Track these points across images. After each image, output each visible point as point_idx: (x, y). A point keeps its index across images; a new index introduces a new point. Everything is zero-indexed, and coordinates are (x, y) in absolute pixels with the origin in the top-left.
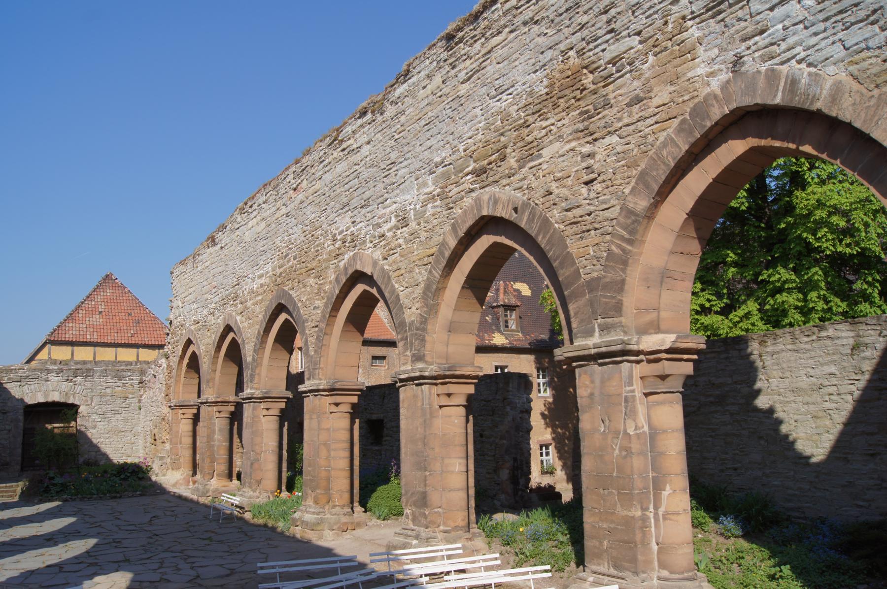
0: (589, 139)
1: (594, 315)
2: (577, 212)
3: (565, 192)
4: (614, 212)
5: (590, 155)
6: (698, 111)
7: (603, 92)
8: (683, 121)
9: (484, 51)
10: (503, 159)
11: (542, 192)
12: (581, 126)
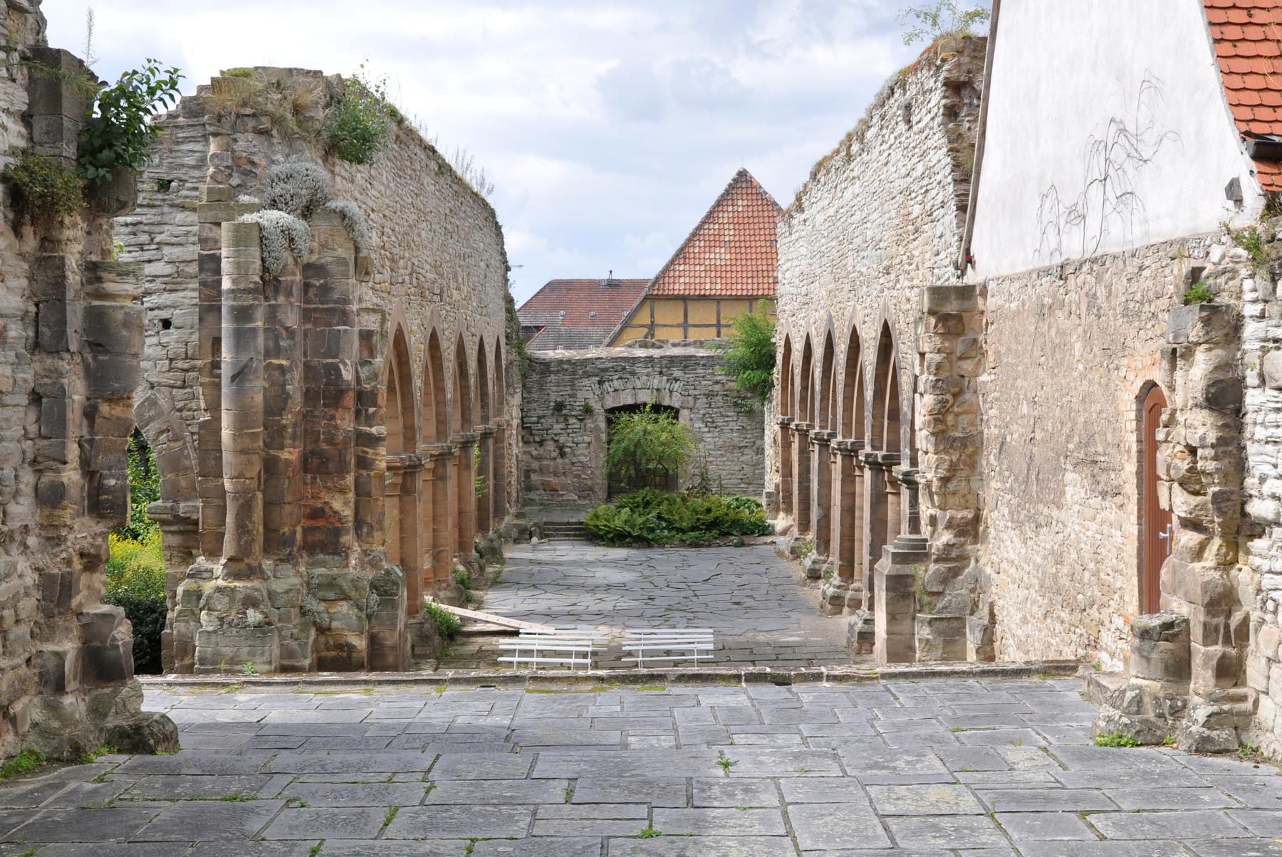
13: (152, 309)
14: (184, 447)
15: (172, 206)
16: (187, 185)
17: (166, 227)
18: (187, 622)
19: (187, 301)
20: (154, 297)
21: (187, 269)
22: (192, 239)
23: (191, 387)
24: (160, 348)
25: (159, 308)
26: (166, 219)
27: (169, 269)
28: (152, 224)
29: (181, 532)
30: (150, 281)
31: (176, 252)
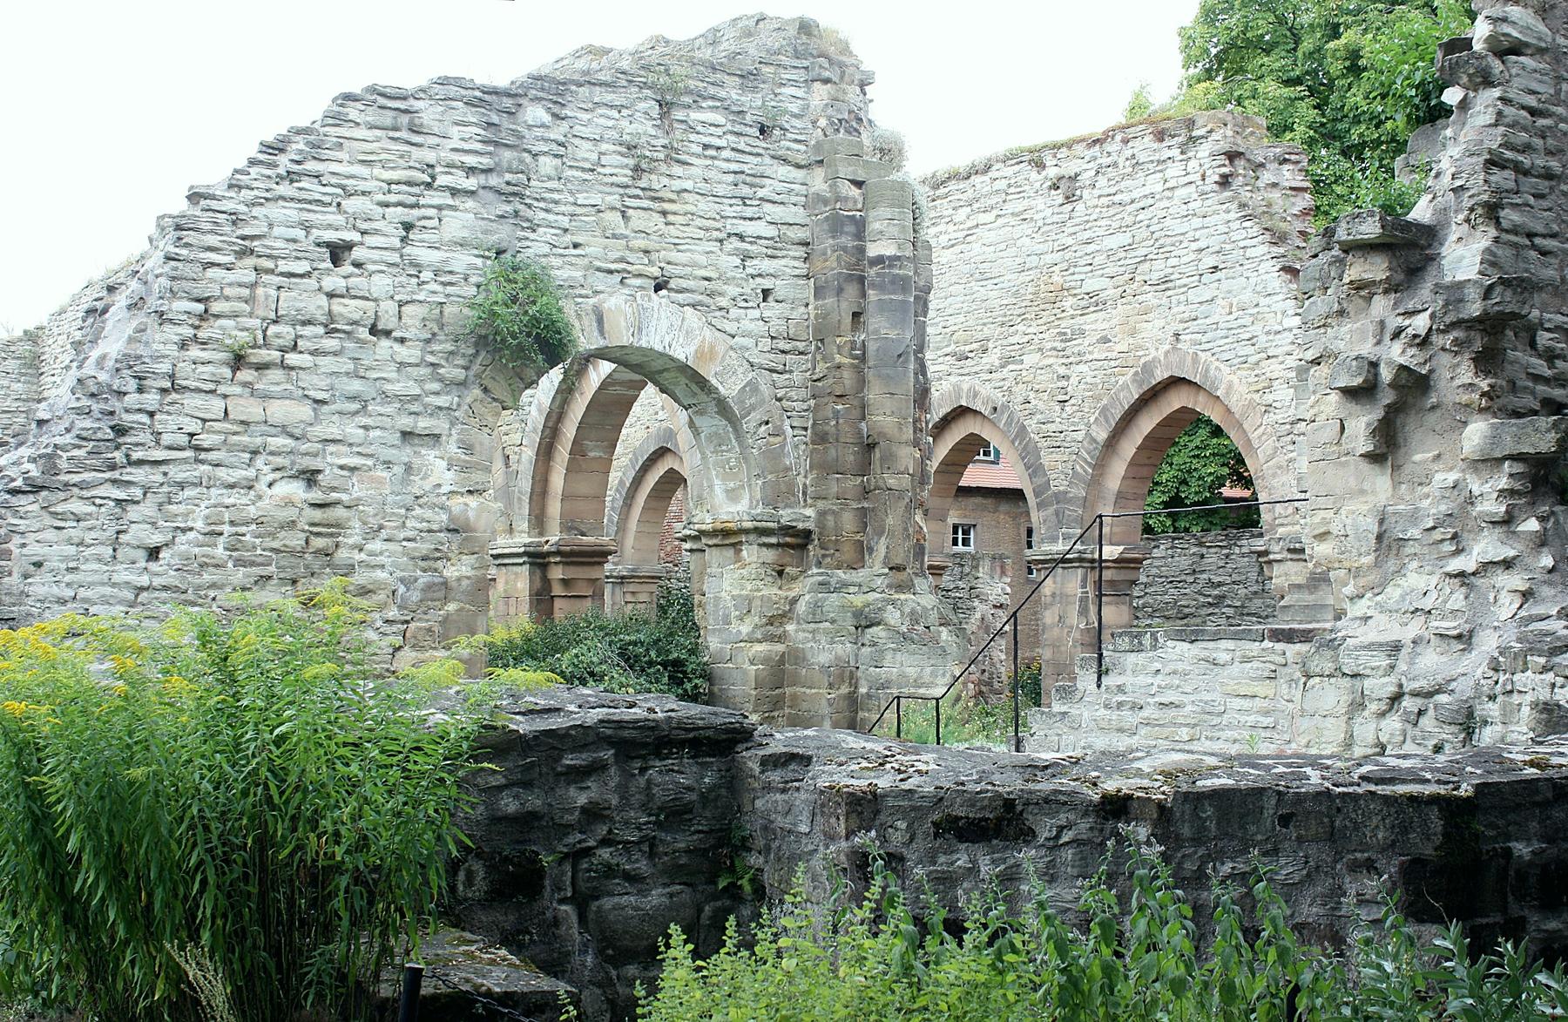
0: (1064, 361)
1: (1060, 524)
2: (1052, 427)
3: (1041, 406)
4: (1080, 436)
5: (1065, 377)
6: (1148, 368)
7: (1080, 320)
8: (1136, 373)
9: (969, 224)
10: (985, 351)
11: (1021, 399)
12: (1059, 345)
13: (753, 277)
14: (783, 446)
15: (773, 157)
16: (789, 135)
20: (755, 262)
22: (794, 199)
27: (771, 231)
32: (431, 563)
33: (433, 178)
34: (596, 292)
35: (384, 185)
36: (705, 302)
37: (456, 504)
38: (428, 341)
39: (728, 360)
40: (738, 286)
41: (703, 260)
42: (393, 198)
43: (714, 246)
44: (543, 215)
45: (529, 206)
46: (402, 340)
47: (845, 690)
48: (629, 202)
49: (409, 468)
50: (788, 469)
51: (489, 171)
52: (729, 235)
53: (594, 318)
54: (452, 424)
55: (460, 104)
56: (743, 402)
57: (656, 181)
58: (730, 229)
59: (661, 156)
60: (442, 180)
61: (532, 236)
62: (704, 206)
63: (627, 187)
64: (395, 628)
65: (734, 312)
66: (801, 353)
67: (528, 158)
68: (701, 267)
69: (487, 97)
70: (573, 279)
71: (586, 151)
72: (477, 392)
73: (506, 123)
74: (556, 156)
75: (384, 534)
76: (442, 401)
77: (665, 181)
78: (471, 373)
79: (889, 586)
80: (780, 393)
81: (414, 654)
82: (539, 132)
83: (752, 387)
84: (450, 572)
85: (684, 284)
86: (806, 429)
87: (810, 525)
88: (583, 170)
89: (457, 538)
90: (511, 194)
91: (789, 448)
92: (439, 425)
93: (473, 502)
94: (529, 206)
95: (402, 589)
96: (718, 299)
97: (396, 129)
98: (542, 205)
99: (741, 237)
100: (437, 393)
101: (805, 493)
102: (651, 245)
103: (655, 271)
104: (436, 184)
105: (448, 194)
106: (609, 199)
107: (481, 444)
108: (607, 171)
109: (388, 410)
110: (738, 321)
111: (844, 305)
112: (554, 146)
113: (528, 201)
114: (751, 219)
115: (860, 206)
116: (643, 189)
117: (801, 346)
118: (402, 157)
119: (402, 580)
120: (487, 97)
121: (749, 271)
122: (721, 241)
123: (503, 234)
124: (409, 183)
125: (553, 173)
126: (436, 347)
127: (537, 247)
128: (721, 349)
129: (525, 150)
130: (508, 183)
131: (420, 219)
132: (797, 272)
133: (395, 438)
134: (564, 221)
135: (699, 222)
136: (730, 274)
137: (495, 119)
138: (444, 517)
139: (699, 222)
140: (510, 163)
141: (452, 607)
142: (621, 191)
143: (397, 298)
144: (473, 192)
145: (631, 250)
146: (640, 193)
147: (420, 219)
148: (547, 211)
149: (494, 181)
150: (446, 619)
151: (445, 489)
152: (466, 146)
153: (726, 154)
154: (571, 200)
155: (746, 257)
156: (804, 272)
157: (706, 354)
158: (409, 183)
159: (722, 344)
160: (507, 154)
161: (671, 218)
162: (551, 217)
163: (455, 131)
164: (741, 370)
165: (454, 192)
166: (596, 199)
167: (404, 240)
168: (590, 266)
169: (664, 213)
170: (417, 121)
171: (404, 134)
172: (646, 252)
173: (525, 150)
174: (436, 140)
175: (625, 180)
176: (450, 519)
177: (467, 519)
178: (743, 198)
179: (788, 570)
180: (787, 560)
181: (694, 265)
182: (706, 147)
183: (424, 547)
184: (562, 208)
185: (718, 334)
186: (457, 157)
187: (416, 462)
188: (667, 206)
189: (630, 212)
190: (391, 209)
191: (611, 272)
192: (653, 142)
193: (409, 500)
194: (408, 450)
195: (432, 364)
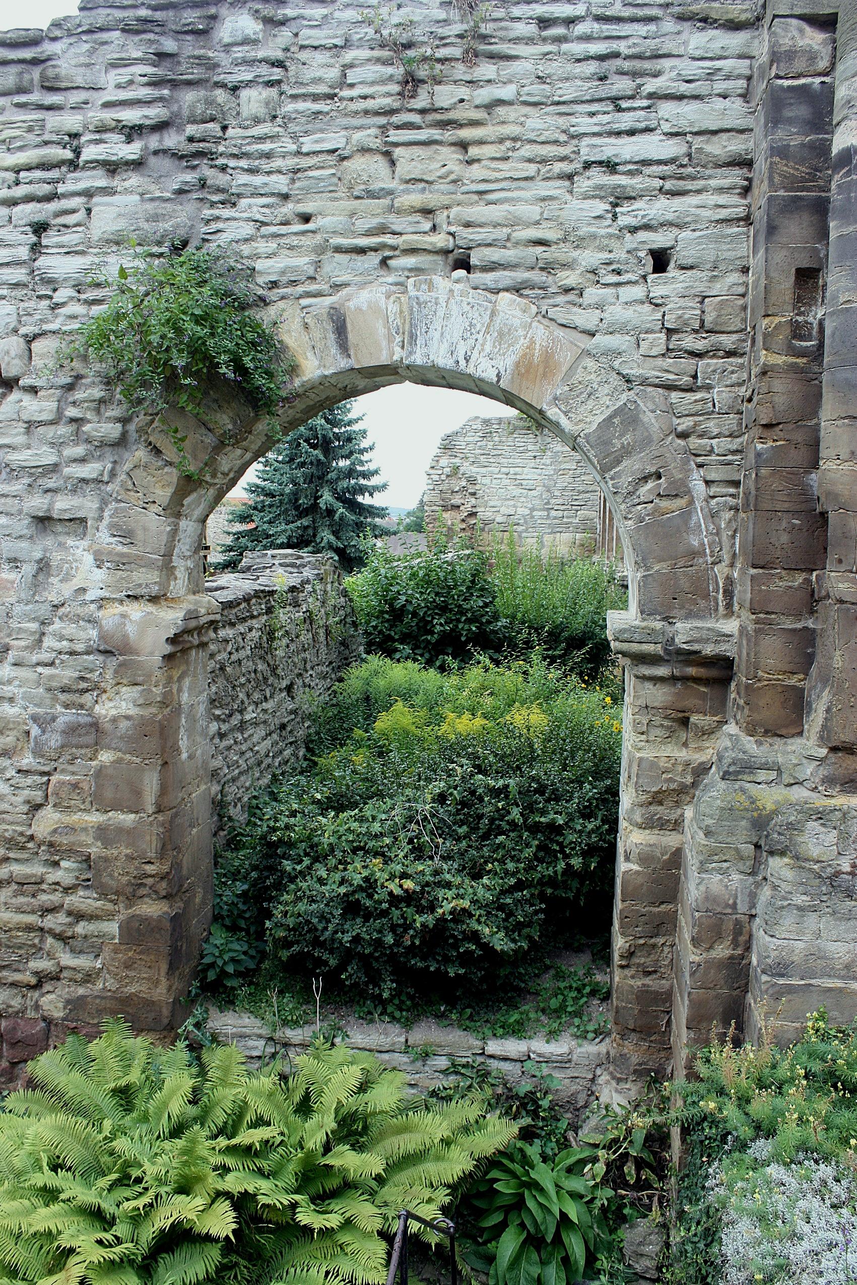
13: (634, 230)
14: (687, 514)
15: (681, 18)
17: (666, 63)
18: (725, 872)
19: (706, 213)
20: (637, 205)
21: (708, 148)
22: (720, 86)
23: (708, 388)
24: (647, 308)
25: (647, 227)
26: (668, 46)
27: (673, 148)
28: (639, 57)
29: (673, 679)
30: (630, 173)
31: (688, 114)
32: (75, 697)
33: (77, 152)
34: (337, 287)
35: (10, 176)
36: (538, 278)
37: (109, 616)
38: (70, 387)
39: (579, 375)
40: (601, 249)
41: (533, 211)
42: (19, 192)
43: (556, 188)
44: (244, 178)
45: (223, 169)
46: (33, 390)
47: (722, 951)
48: (395, 136)
49: (44, 566)
50: (694, 554)
51: (161, 127)
52: (587, 165)
53: (330, 327)
54: (104, 503)
55: (117, 34)
56: (608, 443)
57: (445, 95)
58: (586, 154)
59: (456, 52)
60: (89, 153)
61: (226, 212)
62: (537, 122)
63: (392, 112)
64: (29, 780)
65: (593, 294)
66: (730, 354)
67: (221, 95)
68: (528, 225)
69: (159, 15)
70: (294, 269)
71: (319, 69)
72: (141, 454)
73: (190, 48)
74: (270, 84)
75: (11, 656)
76: (88, 470)
77: (463, 92)
78: (132, 427)
79: (829, 781)
80: (685, 424)
81: (57, 816)
82: (239, 52)
83: (627, 417)
84: (106, 709)
85: (495, 255)
86: (736, 484)
87: (727, 649)
88: (316, 98)
89: (112, 662)
90: (196, 155)
91: (699, 516)
92: (85, 504)
93: (136, 611)
94: (223, 169)
95: (35, 731)
96: (562, 274)
97: (21, 90)
98: (244, 163)
99: (610, 166)
100: (82, 460)
101: (729, 594)
102: (431, 199)
103: (440, 240)
104: (84, 157)
105: (100, 172)
106: (358, 136)
107: (145, 529)
108: (354, 92)
109: (17, 487)
110: (600, 307)
111: (779, 256)
112: (264, 71)
113: (221, 161)
114: (632, 133)
115: (823, 64)
116: (423, 112)
117: (728, 341)
118: (30, 130)
119: (35, 718)
120: (159, 15)
121: (623, 221)
122: (570, 177)
123: (181, 217)
124: (44, 166)
125: (262, 112)
126: (79, 395)
127: (233, 229)
128: (565, 358)
129: (217, 85)
130: (191, 140)
131: (57, 214)
132: (723, 214)
133: (23, 526)
134: (280, 183)
135: (527, 151)
136: (584, 230)
137: (169, 45)
138: (94, 633)
139: (527, 151)
140: (192, 107)
141: (106, 757)
142: (383, 120)
143: (23, 331)
144: (137, 165)
145: (399, 212)
146: (416, 118)
147: (57, 214)
148: (252, 171)
149: (172, 140)
150: (99, 773)
151: (90, 596)
152: (123, 95)
153: (580, 29)
154: (294, 147)
155: (619, 198)
156: (741, 212)
157: (535, 367)
158: (44, 166)
159: (567, 347)
160: (189, 97)
161: (473, 151)
162: (258, 180)
163: (114, 77)
164: (606, 389)
165: (112, 167)
166: (334, 139)
167: (36, 249)
168: (321, 250)
169: (463, 145)
170: (50, 73)
171: (35, 97)
172: (427, 212)
173: (217, 85)
174: (81, 96)
175: (388, 101)
176: (102, 637)
177: (125, 636)
178: (614, 100)
179: (694, 719)
180: (691, 702)
181: (514, 223)
182: (544, 22)
183: (66, 674)
184: (278, 163)
185: (560, 333)
186: (109, 116)
187: (56, 557)
188: (466, 133)
189: (398, 152)
190: (21, 207)
191: (362, 251)
192: (441, 31)
193: (44, 610)
194: (49, 541)
195: (73, 420)
